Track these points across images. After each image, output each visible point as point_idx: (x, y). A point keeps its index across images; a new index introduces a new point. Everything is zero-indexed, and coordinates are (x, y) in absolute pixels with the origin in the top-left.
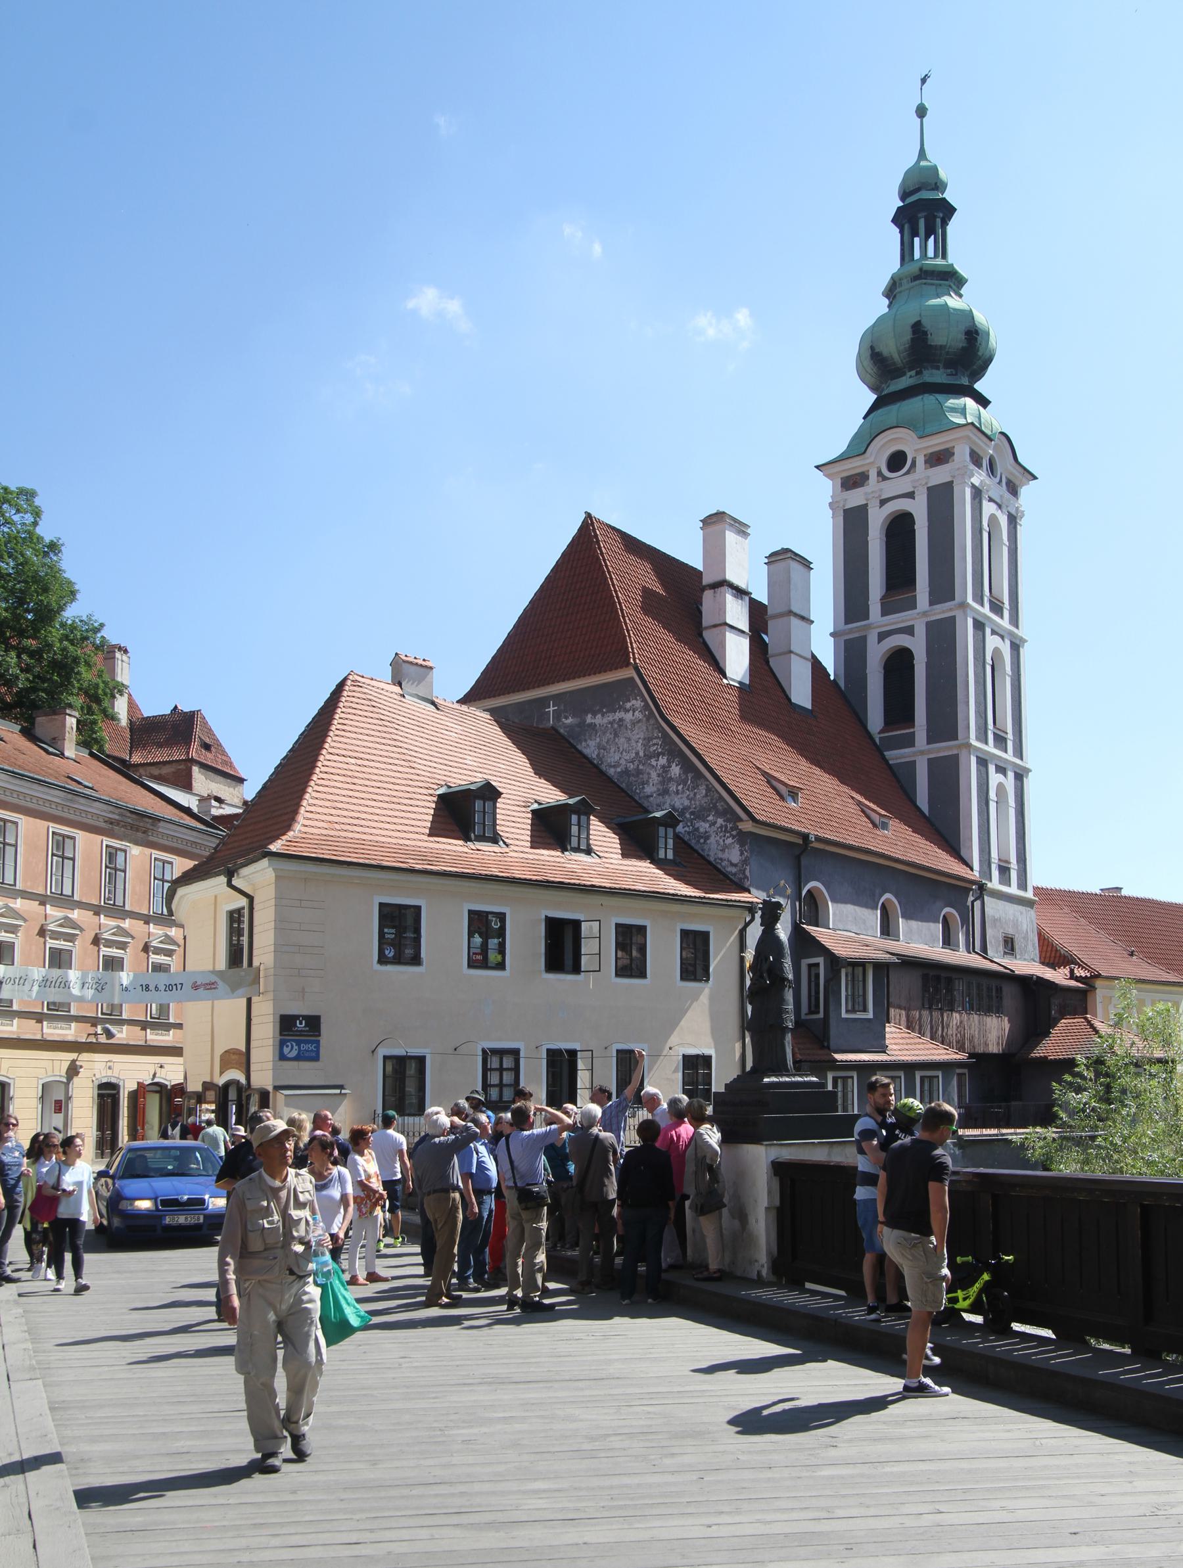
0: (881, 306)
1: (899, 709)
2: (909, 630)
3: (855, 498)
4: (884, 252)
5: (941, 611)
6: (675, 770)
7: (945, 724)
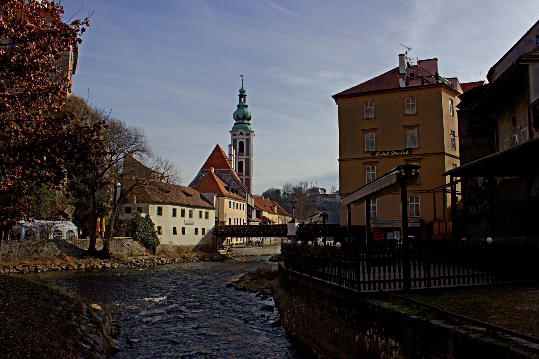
3: (235, 137)
5: (247, 157)
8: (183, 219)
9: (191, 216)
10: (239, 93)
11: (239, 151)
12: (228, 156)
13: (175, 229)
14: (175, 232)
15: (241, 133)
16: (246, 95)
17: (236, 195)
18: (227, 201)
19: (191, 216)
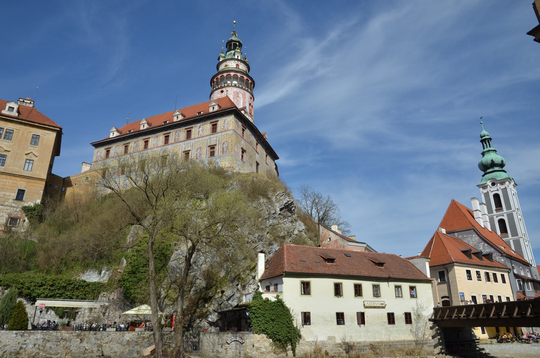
1: (504, 229)
2: (503, 215)
3: (485, 191)
6: (486, 245)
8: (359, 301)
10: (481, 139)
11: (496, 207)
16: (491, 139)
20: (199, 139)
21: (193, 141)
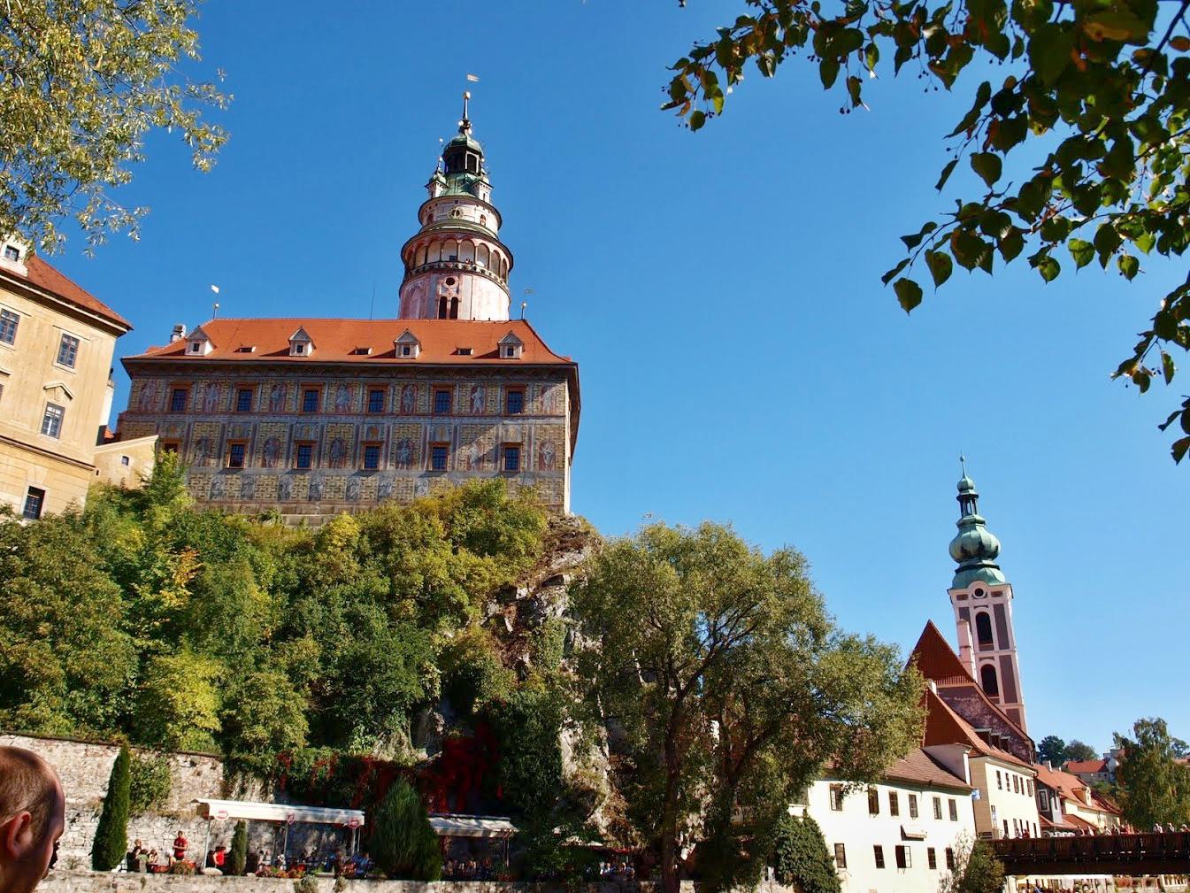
0: (957, 531)
2: (992, 658)
3: (964, 604)
4: (956, 513)
5: (1004, 653)
6: (995, 721)
7: (1012, 696)
8: (896, 822)
9: (914, 814)
10: (958, 493)
12: (956, 651)
13: (878, 850)
14: (880, 863)
15: (979, 592)
16: (977, 496)
17: (1006, 755)
18: (991, 769)
19: (914, 814)
20: (471, 421)
21: (457, 421)
